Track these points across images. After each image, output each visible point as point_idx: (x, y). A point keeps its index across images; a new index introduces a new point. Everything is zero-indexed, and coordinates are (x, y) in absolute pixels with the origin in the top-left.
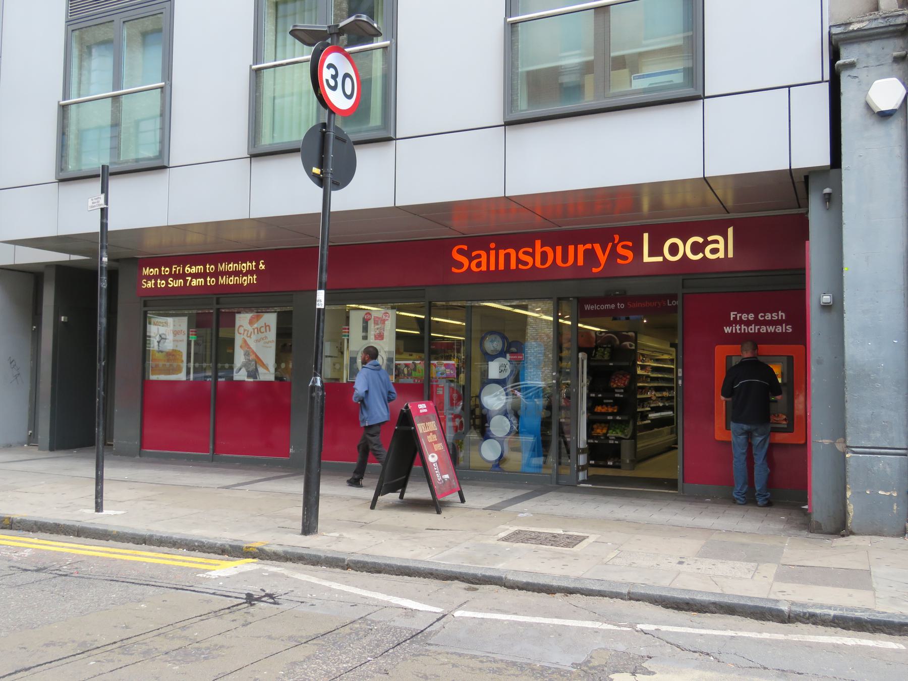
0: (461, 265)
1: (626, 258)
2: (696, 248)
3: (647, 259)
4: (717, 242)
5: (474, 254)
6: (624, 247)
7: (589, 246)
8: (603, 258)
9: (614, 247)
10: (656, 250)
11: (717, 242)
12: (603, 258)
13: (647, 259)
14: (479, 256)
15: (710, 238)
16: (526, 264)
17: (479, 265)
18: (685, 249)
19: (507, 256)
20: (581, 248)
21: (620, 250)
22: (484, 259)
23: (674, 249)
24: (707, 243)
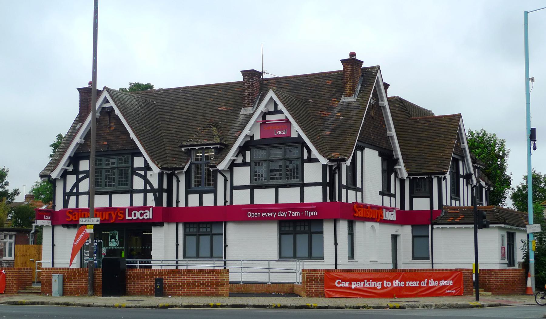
0: (69, 218)
1: (121, 217)
2: (142, 215)
3: (127, 218)
4: (147, 213)
6: (121, 213)
8: (114, 216)
11: (147, 213)
12: (114, 216)
13: (127, 218)
14: (75, 215)
15: (145, 211)
17: (75, 218)
18: (138, 215)
21: (119, 215)
23: (135, 214)
24: (144, 213)
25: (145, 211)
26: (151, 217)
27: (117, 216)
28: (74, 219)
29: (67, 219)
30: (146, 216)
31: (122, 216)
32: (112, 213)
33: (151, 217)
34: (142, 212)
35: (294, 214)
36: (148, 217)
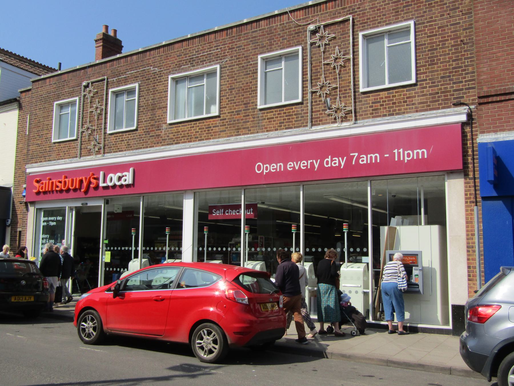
3: (101, 184)
6: (94, 178)
9: (90, 178)
10: (105, 181)
13: (101, 184)
19: (53, 183)
21: (92, 180)
25: (124, 174)
30: (125, 180)
35: (364, 160)
36: (127, 183)
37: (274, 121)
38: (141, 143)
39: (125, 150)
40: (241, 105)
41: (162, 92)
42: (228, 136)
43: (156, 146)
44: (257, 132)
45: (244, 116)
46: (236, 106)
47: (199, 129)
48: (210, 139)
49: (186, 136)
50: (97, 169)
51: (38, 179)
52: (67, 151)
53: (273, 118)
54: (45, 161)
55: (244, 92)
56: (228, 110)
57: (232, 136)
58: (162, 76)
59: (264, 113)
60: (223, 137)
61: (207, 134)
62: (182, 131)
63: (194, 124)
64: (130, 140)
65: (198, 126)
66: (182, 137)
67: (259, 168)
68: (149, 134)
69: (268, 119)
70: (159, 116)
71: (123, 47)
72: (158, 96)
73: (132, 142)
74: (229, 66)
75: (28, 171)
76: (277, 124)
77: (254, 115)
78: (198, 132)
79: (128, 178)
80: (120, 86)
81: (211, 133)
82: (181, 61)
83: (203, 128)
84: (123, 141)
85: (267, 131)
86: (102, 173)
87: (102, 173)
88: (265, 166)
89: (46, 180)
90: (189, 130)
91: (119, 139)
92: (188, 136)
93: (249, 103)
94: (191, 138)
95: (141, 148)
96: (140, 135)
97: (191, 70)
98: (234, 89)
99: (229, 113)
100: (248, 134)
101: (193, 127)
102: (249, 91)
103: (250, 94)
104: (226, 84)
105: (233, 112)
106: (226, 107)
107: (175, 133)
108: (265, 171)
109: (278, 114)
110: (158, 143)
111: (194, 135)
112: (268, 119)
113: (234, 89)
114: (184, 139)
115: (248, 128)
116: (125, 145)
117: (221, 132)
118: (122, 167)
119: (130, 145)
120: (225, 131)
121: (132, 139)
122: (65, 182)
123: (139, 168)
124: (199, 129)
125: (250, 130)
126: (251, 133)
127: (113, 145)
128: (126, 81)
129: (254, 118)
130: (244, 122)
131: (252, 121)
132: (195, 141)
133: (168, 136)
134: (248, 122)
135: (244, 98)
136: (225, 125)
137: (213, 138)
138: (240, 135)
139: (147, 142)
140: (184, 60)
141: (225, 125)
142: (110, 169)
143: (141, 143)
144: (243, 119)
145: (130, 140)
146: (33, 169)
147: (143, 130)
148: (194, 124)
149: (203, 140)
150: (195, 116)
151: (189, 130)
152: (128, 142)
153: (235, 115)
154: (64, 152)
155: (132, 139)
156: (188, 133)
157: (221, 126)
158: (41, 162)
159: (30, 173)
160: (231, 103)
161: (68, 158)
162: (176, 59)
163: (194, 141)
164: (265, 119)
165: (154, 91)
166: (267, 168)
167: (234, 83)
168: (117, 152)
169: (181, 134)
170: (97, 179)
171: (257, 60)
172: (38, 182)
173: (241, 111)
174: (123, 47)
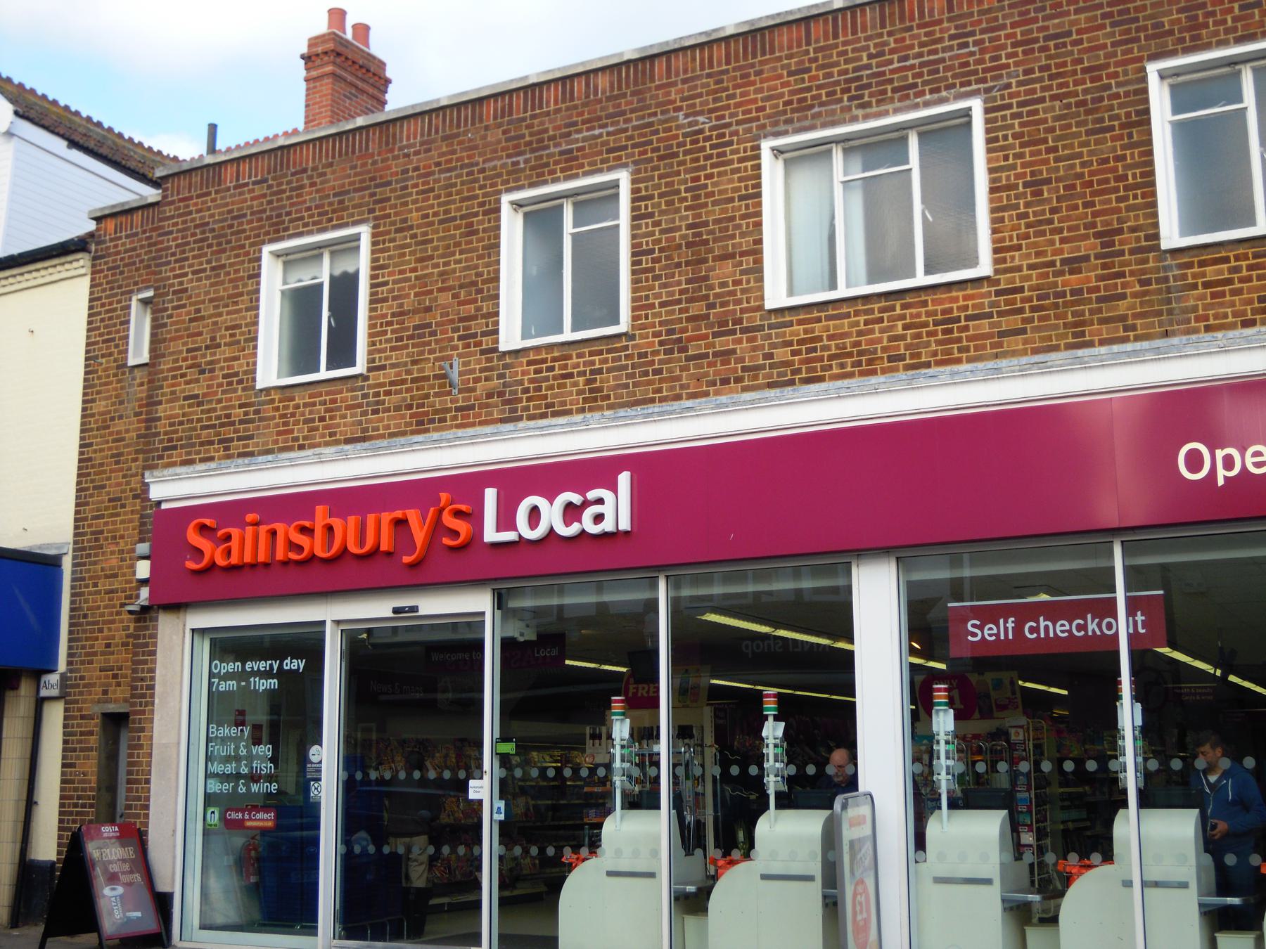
0: (199, 552)
1: (455, 534)
2: (572, 513)
3: (491, 534)
4: (600, 501)
5: (220, 533)
6: (458, 514)
7: (398, 514)
8: (419, 535)
9: (441, 511)
11: (600, 501)
12: (419, 535)
13: (491, 534)
14: (228, 538)
15: (592, 495)
16: (300, 549)
18: (552, 515)
19: (273, 533)
20: (386, 517)
21: (449, 521)
22: (234, 544)
23: (534, 513)
24: (586, 504)
25: (592, 495)
26: (625, 525)
27: (438, 528)
28: (221, 562)
29: (191, 565)
30: (599, 518)
31: (462, 527)
32: (413, 515)
33: (625, 525)
34: (576, 498)
36: (607, 526)
37: (1235, 293)
38: (650, 383)
39: (582, 410)
40: (1086, 237)
41: (732, 200)
42: (1036, 351)
43: (717, 393)
44: (1166, 334)
45: (1100, 278)
46: (1063, 241)
47: (905, 327)
48: (958, 361)
49: (850, 355)
50: (467, 486)
51: (208, 521)
52: (322, 419)
53: (1229, 282)
54: (229, 457)
55: (1094, 194)
56: (1028, 256)
57: (1055, 348)
58: (730, 143)
59: (1189, 265)
60: (1014, 354)
61: (939, 343)
62: (830, 338)
63: (882, 310)
64: (600, 371)
65: (903, 317)
66: (831, 358)
67: (1194, 461)
68: (682, 350)
69: (1206, 285)
70: (723, 285)
71: (388, 81)
72: (713, 213)
73: (607, 381)
74: (1020, 104)
75: (156, 493)
76: (1250, 302)
77: (1144, 272)
78: (903, 337)
79: (615, 509)
80: (545, 183)
81: (959, 340)
82: (809, 89)
83: (926, 325)
84: (571, 375)
85: (1208, 329)
86: (490, 495)
87: (490, 495)
88: (1220, 454)
89: (242, 525)
90: (860, 333)
91: (551, 369)
92: (860, 353)
93: (1120, 231)
94: (870, 362)
95: (652, 401)
96: (640, 356)
97: (854, 119)
98: (1048, 181)
99: (1031, 267)
100: (1124, 340)
101: (881, 320)
102: (1116, 190)
103: (1119, 200)
104: (1013, 167)
105: (1052, 264)
106: (1019, 248)
107: (800, 342)
108: (1221, 474)
109: (1250, 268)
110: (725, 381)
111: (884, 349)
112: (1206, 285)
113: (1048, 181)
114: (842, 366)
115: (1123, 318)
116: (580, 392)
117: (1002, 334)
118: (594, 472)
119: (600, 390)
120: (1023, 331)
121: (609, 370)
122: (330, 529)
123: (654, 472)
124: (905, 327)
125: (1134, 328)
126: (1137, 339)
127: (526, 391)
128: (571, 164)
129: (1143, 283)
130: (1099, 300)
131: (1135, 295)
132: (895, 370)
133: (771, 356)
134: (1123, 297)
135: (1095, 215)
136: (1021, 311)
137: (969, 360)
138: (1090, 344)
139: (679, 378)
140: (819, 87)
141: (1021, 311)
142: (518, 481)
143: (650, 383)
144: (1097, 289)
145: (600, 371)
146: (174, 488)
147: (655, 335)
148: (882, 310)
149: (927, 365)
150: (871, 280)
151: (860, 333)
152: (588, 382)
153: (1061, 273)
154: (306, 421)
155: (609, 370)
156: (858, 344)
157: (1000, 314)
158: (211, 459)
159: (159, 503)
160: (1043, 233)
161: (327, 444)
162: (783, 85)
163: (884, 371)
164: (1195, 286)
165: (696, 198)
166: (1229, 463)
167: (1046, 162)
168: (543, 416)
169: (824, 348)
170: (475, 517)
171: (1144, 79)
172: (203, 529)
173: (1086, 258)
174: (388, 81)
